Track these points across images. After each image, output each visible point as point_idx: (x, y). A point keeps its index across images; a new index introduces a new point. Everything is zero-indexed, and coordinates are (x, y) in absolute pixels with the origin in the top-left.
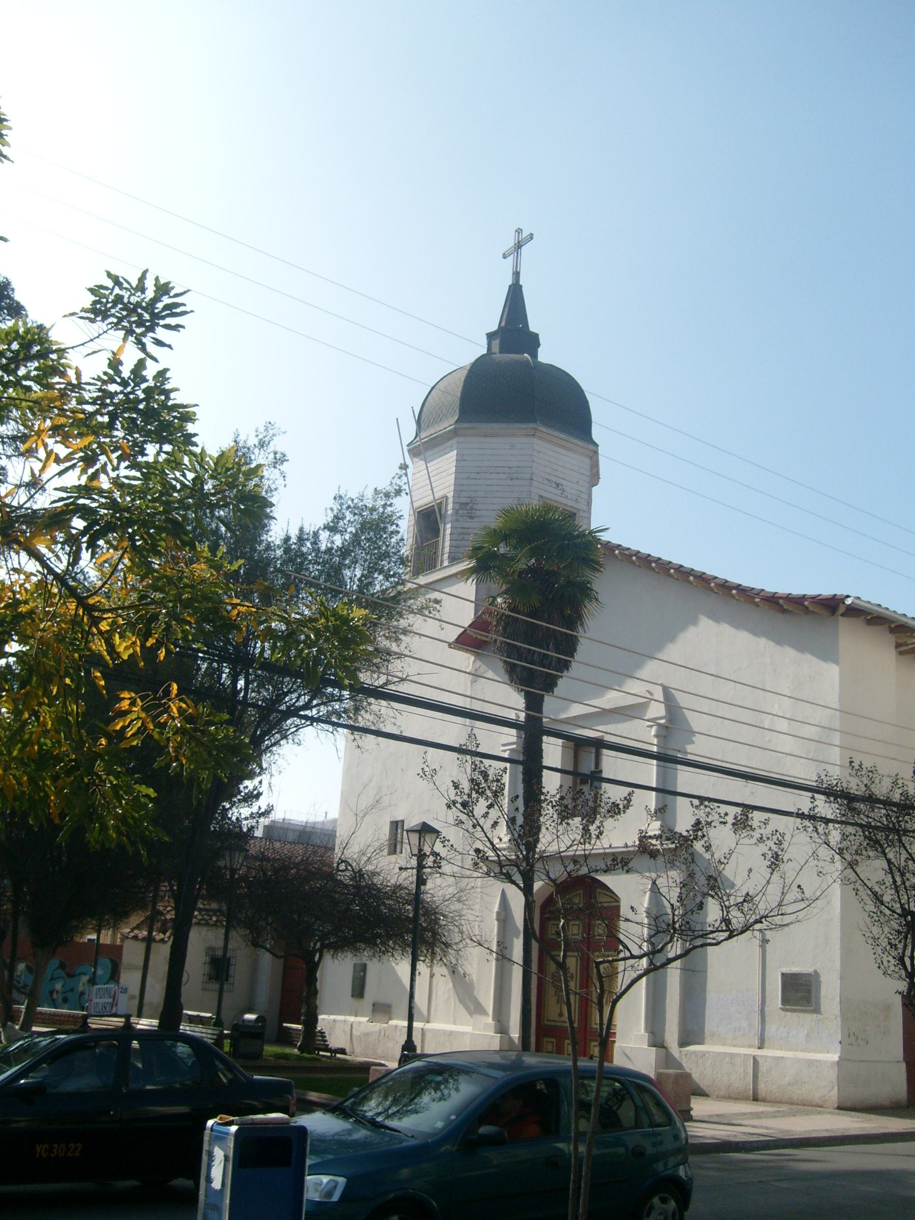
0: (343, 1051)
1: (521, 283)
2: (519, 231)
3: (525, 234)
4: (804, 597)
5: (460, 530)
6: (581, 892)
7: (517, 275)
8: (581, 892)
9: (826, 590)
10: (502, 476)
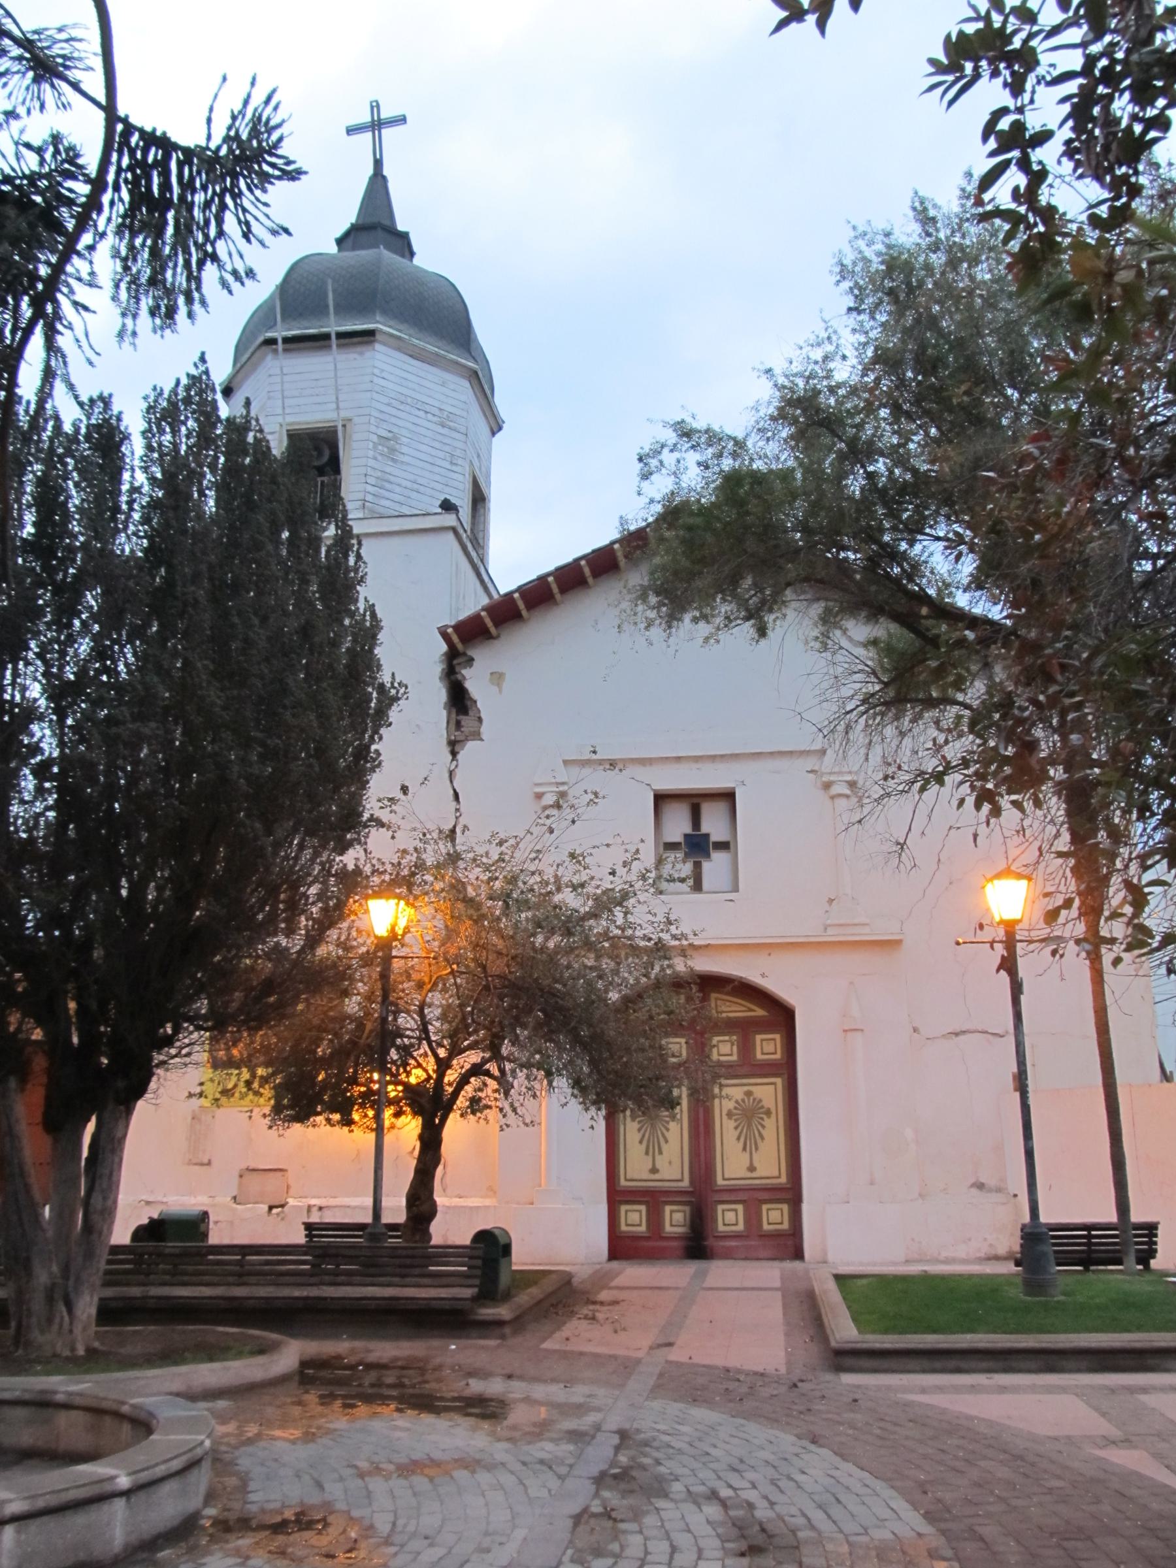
2: (375, 106)
5: (379, 474)
7: (378, 164)
10: (430, 416)
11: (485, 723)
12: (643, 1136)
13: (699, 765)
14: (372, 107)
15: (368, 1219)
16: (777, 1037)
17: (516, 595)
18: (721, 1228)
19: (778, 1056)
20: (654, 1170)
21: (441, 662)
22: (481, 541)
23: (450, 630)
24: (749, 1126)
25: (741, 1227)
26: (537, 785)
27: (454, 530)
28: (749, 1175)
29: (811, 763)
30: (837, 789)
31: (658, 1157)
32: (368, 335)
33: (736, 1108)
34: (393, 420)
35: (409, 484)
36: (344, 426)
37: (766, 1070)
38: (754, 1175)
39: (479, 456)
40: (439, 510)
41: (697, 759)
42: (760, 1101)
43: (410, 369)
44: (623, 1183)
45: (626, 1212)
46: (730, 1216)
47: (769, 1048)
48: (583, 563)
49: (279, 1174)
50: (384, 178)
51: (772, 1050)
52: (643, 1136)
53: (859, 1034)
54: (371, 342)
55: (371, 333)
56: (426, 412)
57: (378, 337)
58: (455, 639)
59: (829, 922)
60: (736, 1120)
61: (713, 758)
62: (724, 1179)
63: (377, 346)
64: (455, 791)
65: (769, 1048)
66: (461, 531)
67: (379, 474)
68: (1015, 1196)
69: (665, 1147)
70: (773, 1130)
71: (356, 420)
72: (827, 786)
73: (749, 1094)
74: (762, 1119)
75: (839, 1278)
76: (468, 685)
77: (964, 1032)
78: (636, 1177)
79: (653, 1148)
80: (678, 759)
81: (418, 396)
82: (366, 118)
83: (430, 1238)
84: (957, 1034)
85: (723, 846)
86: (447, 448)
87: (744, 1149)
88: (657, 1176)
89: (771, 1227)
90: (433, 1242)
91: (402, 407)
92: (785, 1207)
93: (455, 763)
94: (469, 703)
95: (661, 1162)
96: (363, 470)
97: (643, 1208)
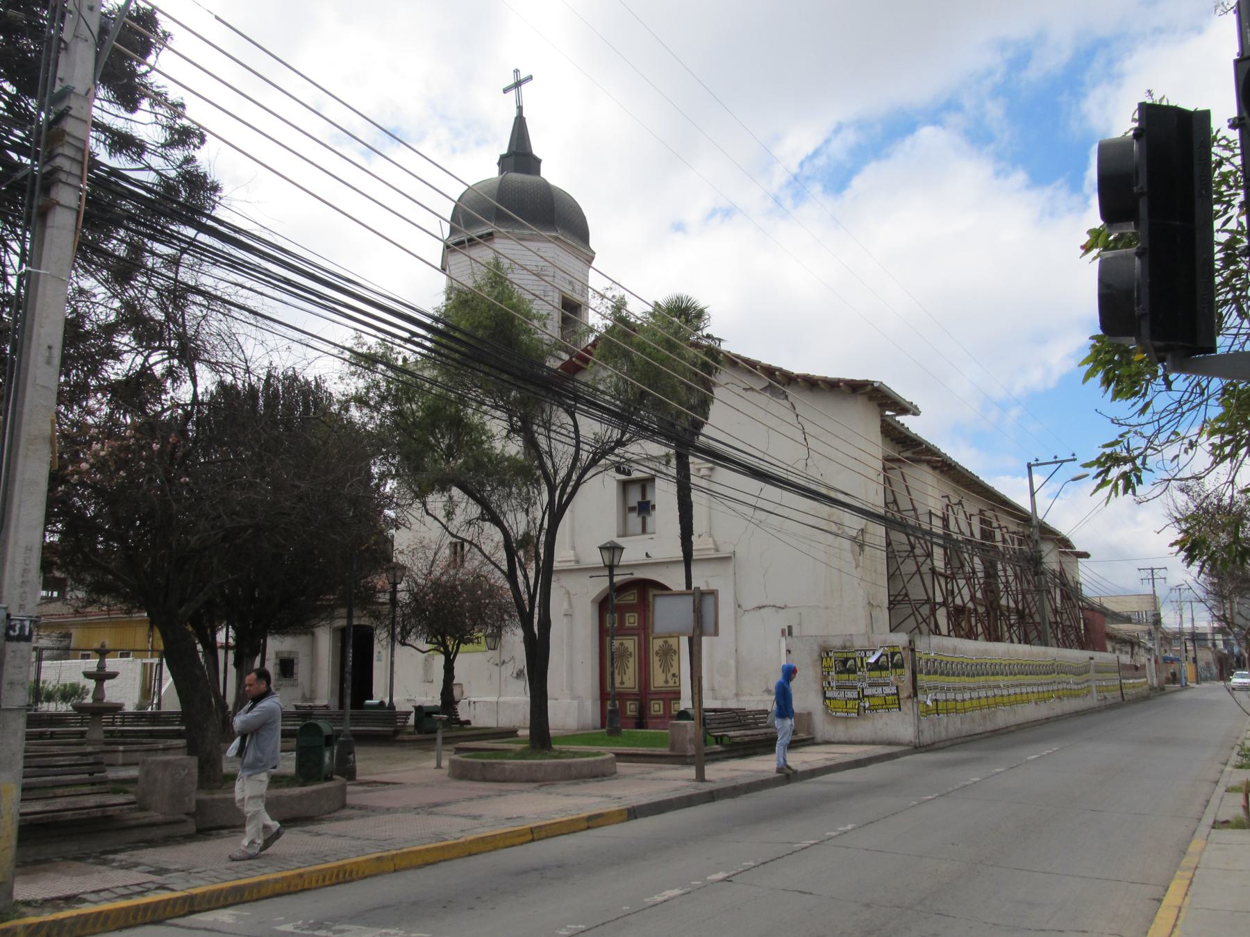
0: (468, 722)
1: (524, 115)
3: (523, 76)
4: (839, 380)
6: (636, 591)
7: (520, 108)
8: (636, 591)
9: (859, 376)
20: (622, 683)
24: (666, 660)
25: (661, 712)
28: (665, 685)
32: (489, 236)
46: (657, 707)
54: (493, 239)
55: (491, 234)
57: (495, 235)
63: (496, 240)
69: (627, 671)
82: (512, 82)
84: (760, 608)
95: (625, 678)
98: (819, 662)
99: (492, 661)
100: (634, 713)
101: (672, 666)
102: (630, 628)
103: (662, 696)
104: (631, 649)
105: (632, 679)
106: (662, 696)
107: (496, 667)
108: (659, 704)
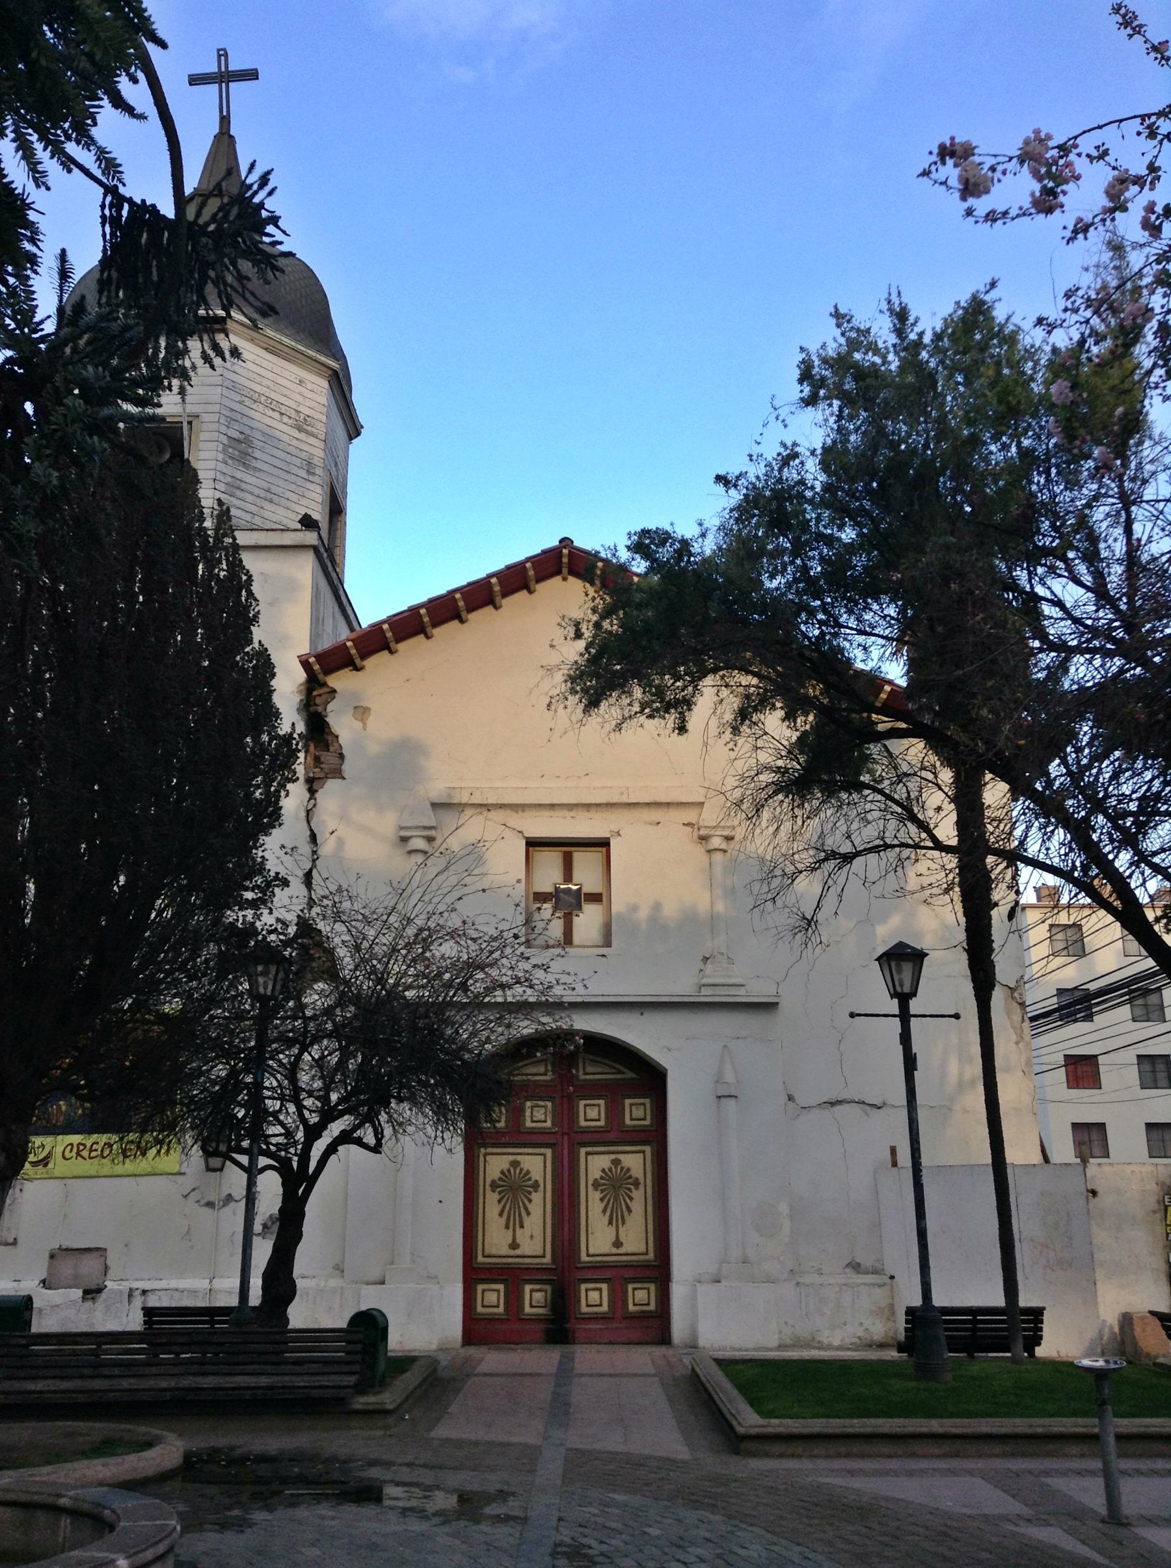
5: (229, 480)
7: (225, 121)
10: (285, 419)
11: (346, 761)
12: (504, 1206)
13: (572, 814)
14: (219, 56)
15: (234, 1302)
16: (647, 1101)
17: (385, 626)
18: (584, 1309)
19: (647, 1122)
20: (514, 1245)
21: (299, 692)
22: (337, 558)
23: (312, 660)
24: (616, 1199)
26: (401, 828)
27: (315, 549)
28: (615, 1251)
29: (690, 816)
30: (716, 842)
31: (519, 1231)
33: (602, 1178)
34: (245, 420)
35: (262, 494)
36: (190, 423)
37: (635, 1137)
38: (622, 1250)
39: (336, 465)
40: (299, 526)
41: (572, 807)
42: (628, 1170)
43: (265, 363)
44: (480, 1259)
45: (484, 1291)
47: (638, 1112)
48: (458, 596)
49: (95, 1254)
50: (232, 137)
51: (642, 1116)
52: (504, 1206)
53: (732, 1102)
56: (282, 414)
58: (316, 667)
59: (704, 981)
60: (602, 1191)
61: (588, 806)
62: (588, 1255)
64: (311, 830)
65: (638, 1112)
66: (322, 550)
67: (229, 480)
68: (892, 1277)
69: (527, 1221)
70: (639, 1204)
71: (205, 417)
72: (704, 839)
73: (616, 1162)
74: (630, 1190)
75: (719, 1362)
76: (331, 720)
77: (839, 1102)
78: (494, 1252)
79: (514, 1220)
80: (552, 806)
81: (273, 395)
83: (287, 1321)
84: (833, 1104)
85: (595, 898)
86: (304, 455)
87: (610, 1223)
88: (518, 1252)
89: (637, 1308)
90: (290, 1327)
91: (255, 406)
92: (652, 1287)
93: (312, 802)
94: (330, 738)
95: (522, 1236)
96: (212, 475)
97: (501, 1287)
98: (1159, 1216)
99: (194, 1196)
100: (541, 1311)
101: (630, 1211)
102: (533, 1132)
103: (607, 1274)
104: (537, 1174)
105: (538, 1233)
106: (607, 1274)
107: (207, 1210)
108: (600, 1290)
